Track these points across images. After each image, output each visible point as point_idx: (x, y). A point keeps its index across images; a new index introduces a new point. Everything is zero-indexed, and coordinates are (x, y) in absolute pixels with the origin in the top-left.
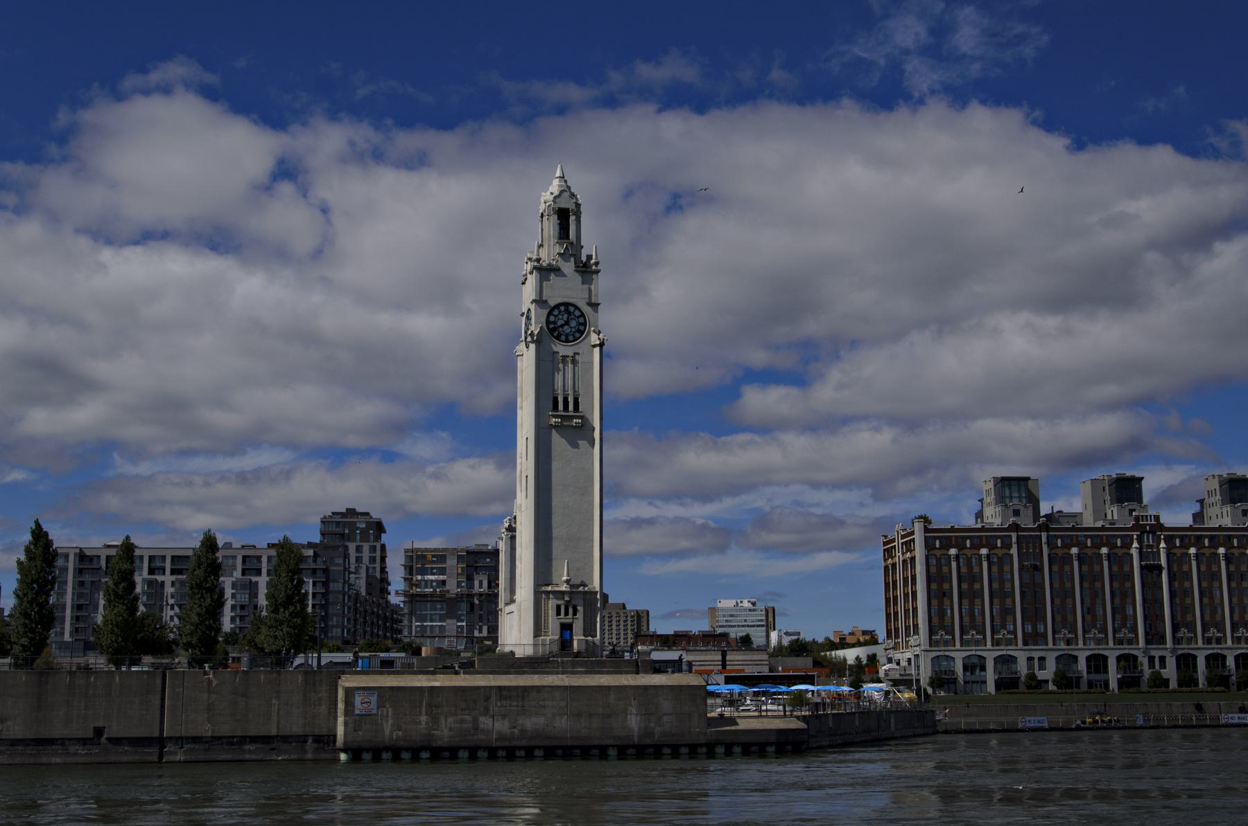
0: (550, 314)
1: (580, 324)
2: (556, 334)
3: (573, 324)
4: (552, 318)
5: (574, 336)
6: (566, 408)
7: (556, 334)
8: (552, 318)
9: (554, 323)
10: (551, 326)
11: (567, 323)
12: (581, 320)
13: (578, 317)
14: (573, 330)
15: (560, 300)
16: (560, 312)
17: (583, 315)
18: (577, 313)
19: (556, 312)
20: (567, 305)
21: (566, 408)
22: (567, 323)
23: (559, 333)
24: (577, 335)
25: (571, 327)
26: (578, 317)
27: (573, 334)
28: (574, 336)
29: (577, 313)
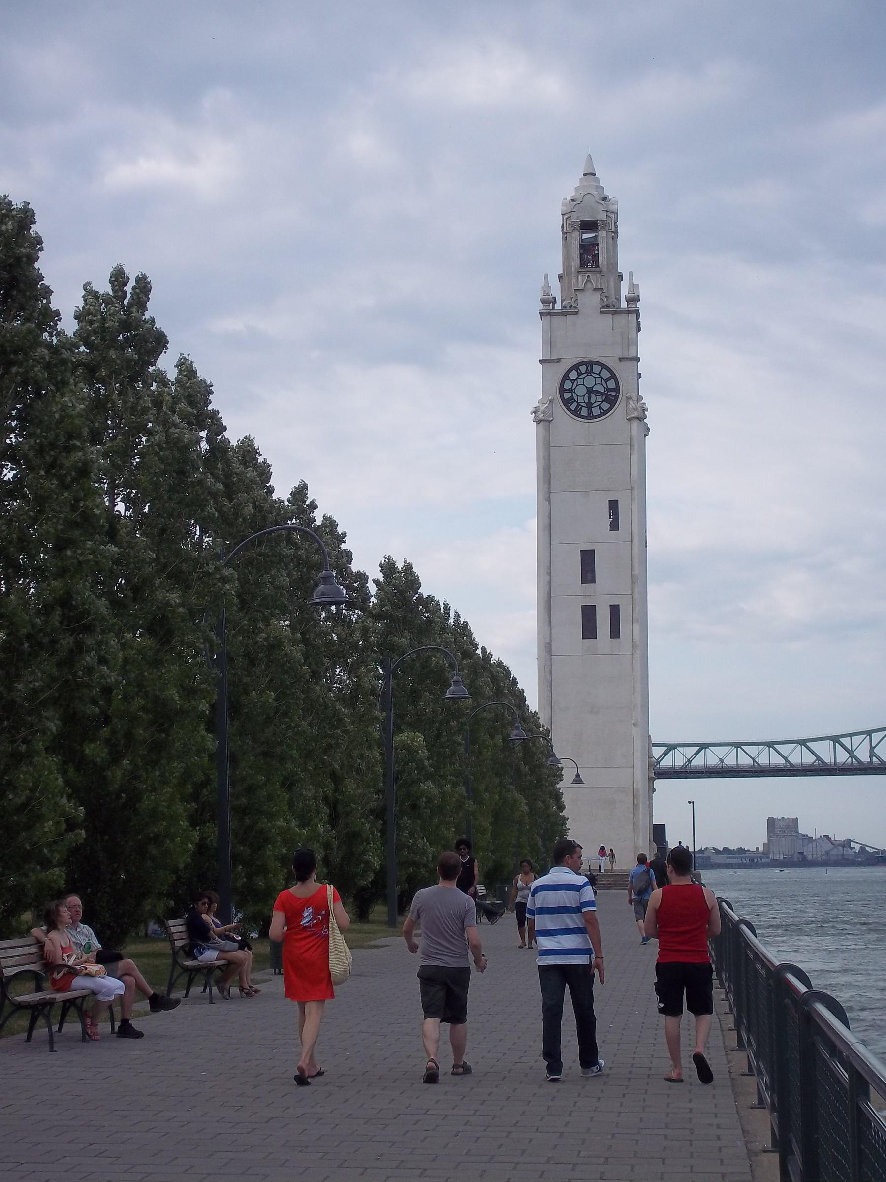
0: (566, 377)
2: (573, 407)
4: (568, 385)
5: (600, 408)
8: (568, 385)
9: (571, 390)
10: (567, 396)
12: (611, 384)
13: (607, 380)
15: (582, 355)
16: (580, 374)
17: (613, 376)
18: (606, 374)
19: (573, 375)
20: (590, 364)
23: (579, 405)
26: (607, 380)
27: (599, 405)
28: (600, 408)
29: (606, 374)
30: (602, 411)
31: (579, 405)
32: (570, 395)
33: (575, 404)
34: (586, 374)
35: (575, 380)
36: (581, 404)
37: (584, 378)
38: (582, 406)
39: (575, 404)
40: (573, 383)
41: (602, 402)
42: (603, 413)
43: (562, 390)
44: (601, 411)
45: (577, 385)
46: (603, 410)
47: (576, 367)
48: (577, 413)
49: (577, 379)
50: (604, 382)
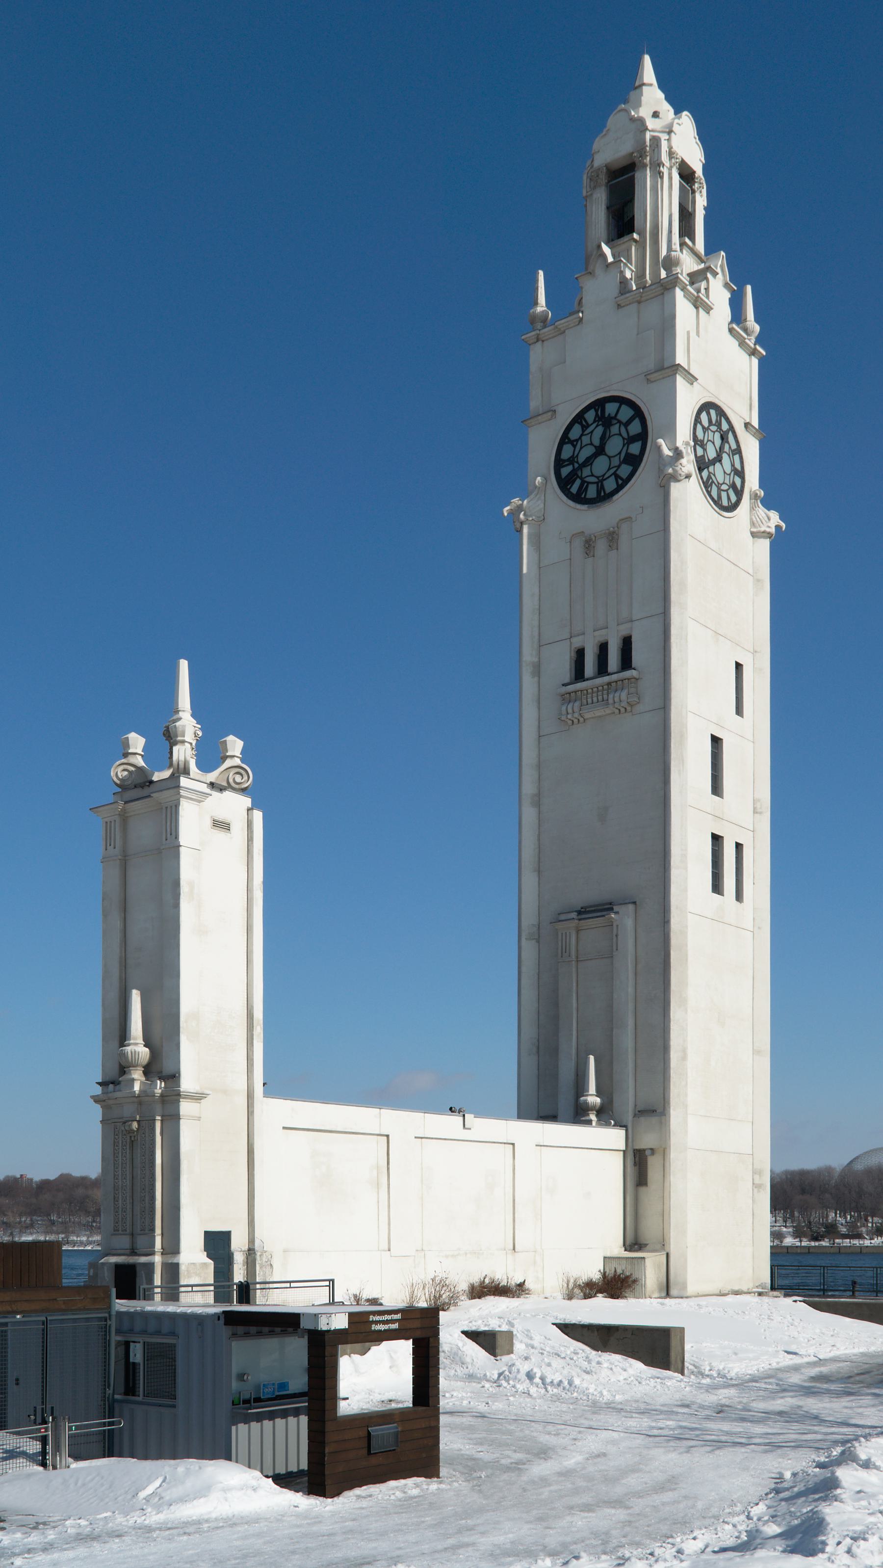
0: (565, 439)
1: (631, 440)
2: (574, 489)
3: (614, 446)
5: (617, 477)
6: (602, 668)
7: (574, 489)
9: (572, 460)
10: (565, 471)
11: (600, 450)
12: (635, 428)
13: (627, 424)
14: (616, 461)
16: (584, 428)
18: (626, 413)
20: (599, 404)
21: (602, 668)
22: (600, 450)
23: (583, 482)
24: (624, 471)
25: (609, 457)
27: (615, 474)
28: (617, 477)
29: (626, 413)
30: (620, 482)
31: (581, 478)
32: (570, 468)
33: (578, 482)
34: (595, 425)
35: (577, 440)
36: (588, 479)
37: (592, 432)
38: (589, 483)
39: (578, 482)
40: (575, 446)
41: (619, 467)
42: (622, 483)
43: (559, 463)
44: (617, 483)
45: (581, 448)
46: (622, 479)
47: (579, 418)
48: (579, 498)
49: (580, 438)
50: (623, 429)
